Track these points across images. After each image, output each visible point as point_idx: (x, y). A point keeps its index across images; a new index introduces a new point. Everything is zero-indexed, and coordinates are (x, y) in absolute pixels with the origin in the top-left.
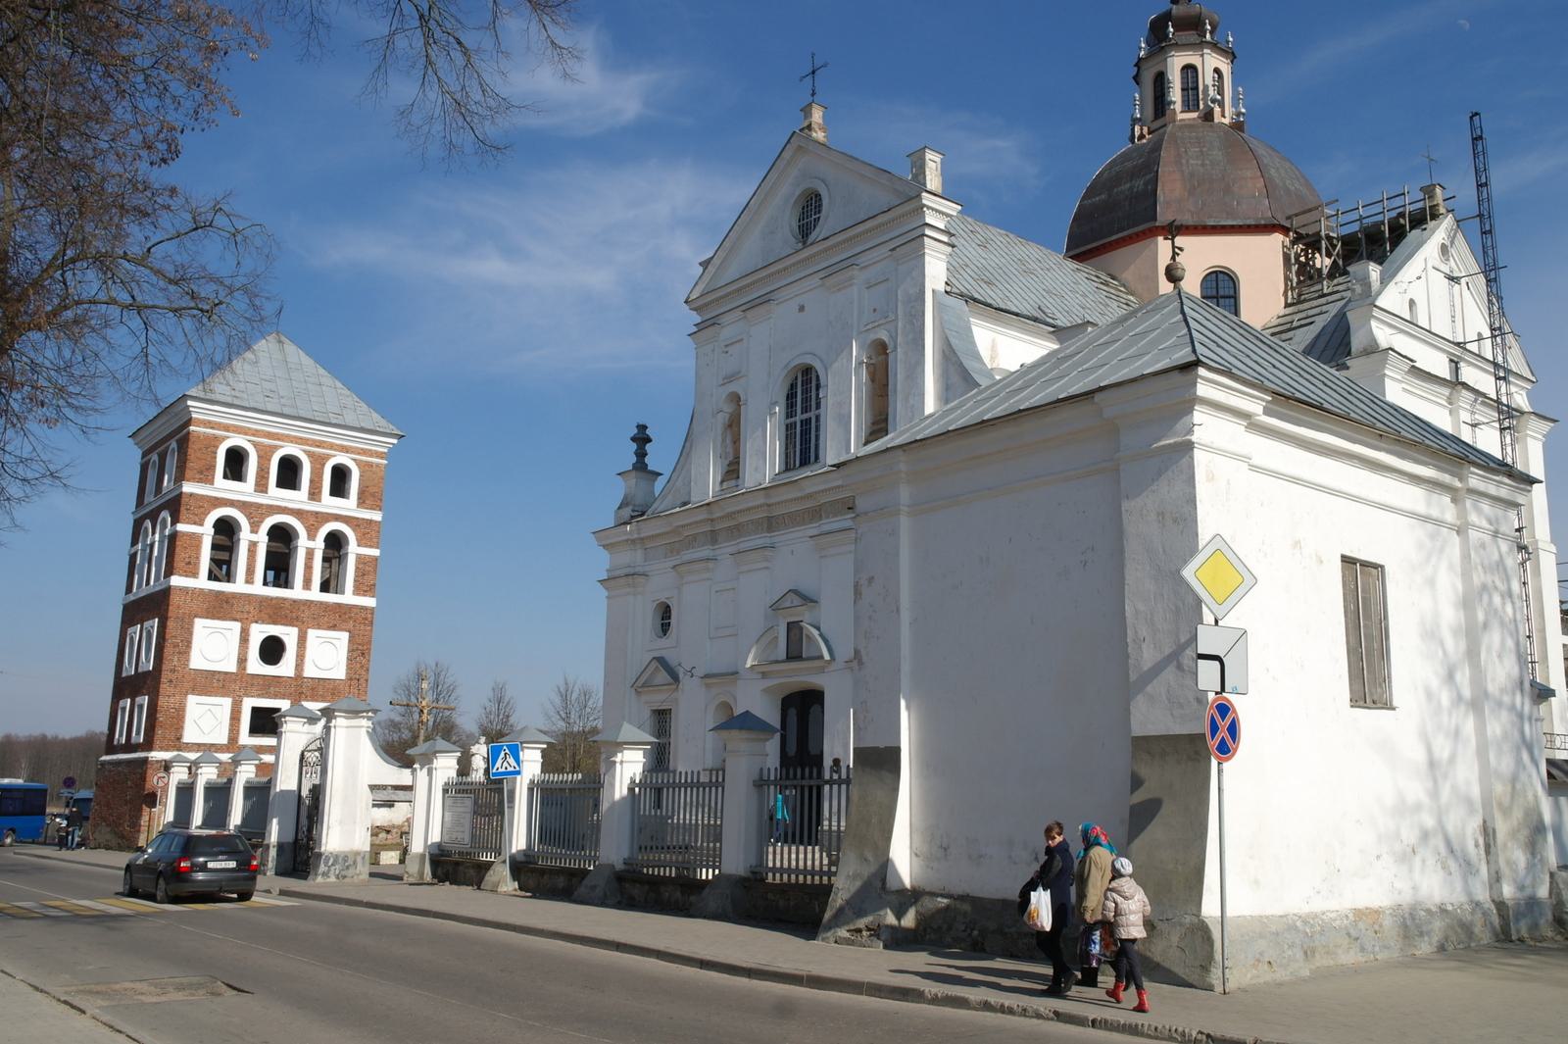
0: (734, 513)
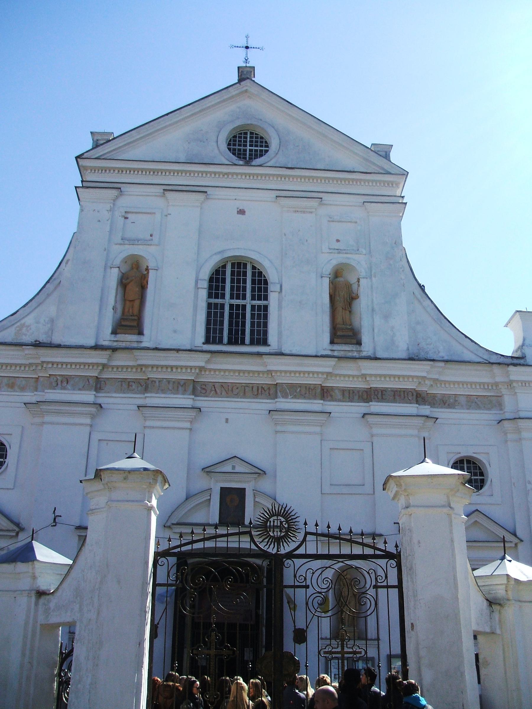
0: (147, 366)
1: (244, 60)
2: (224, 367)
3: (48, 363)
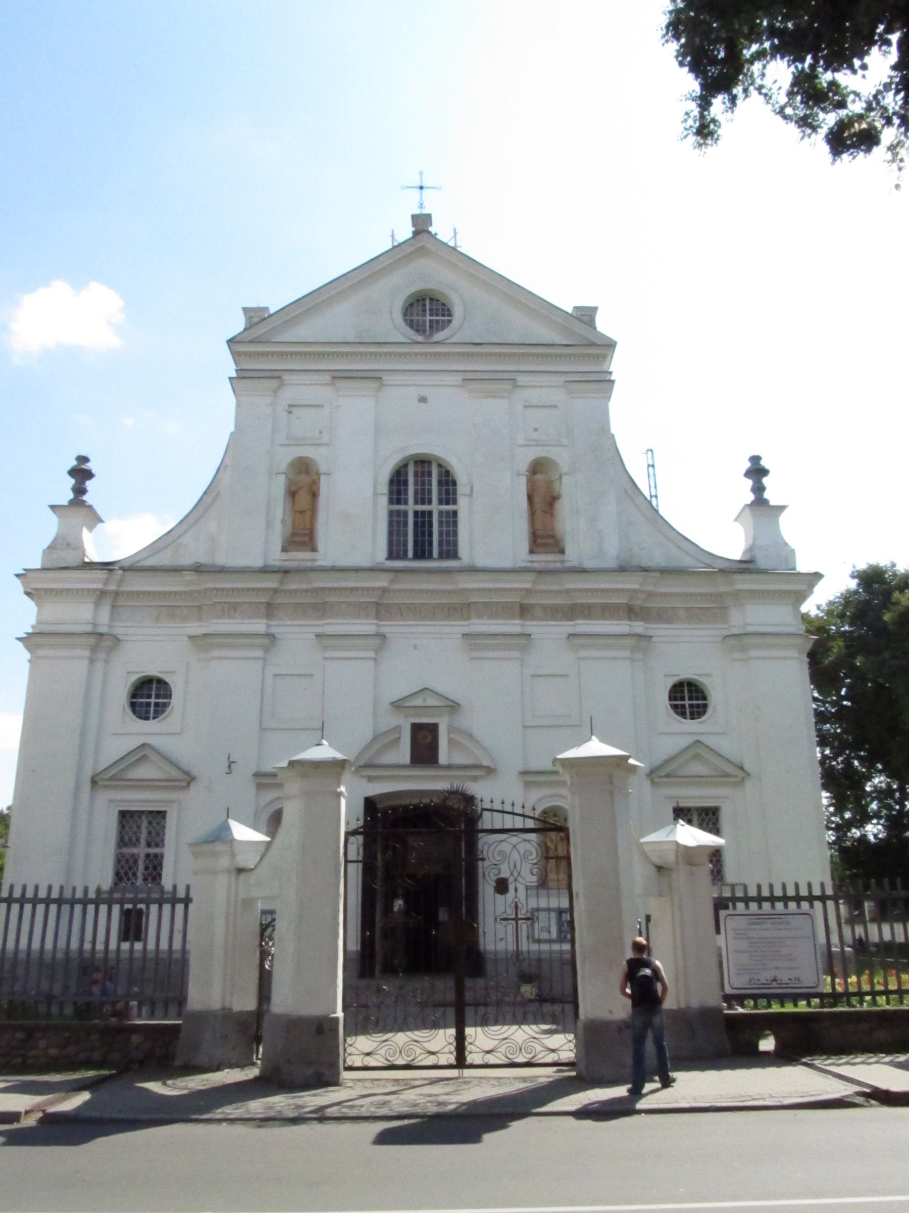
1: (418, 204)
2: (410, 586)
3: (211, 590)
